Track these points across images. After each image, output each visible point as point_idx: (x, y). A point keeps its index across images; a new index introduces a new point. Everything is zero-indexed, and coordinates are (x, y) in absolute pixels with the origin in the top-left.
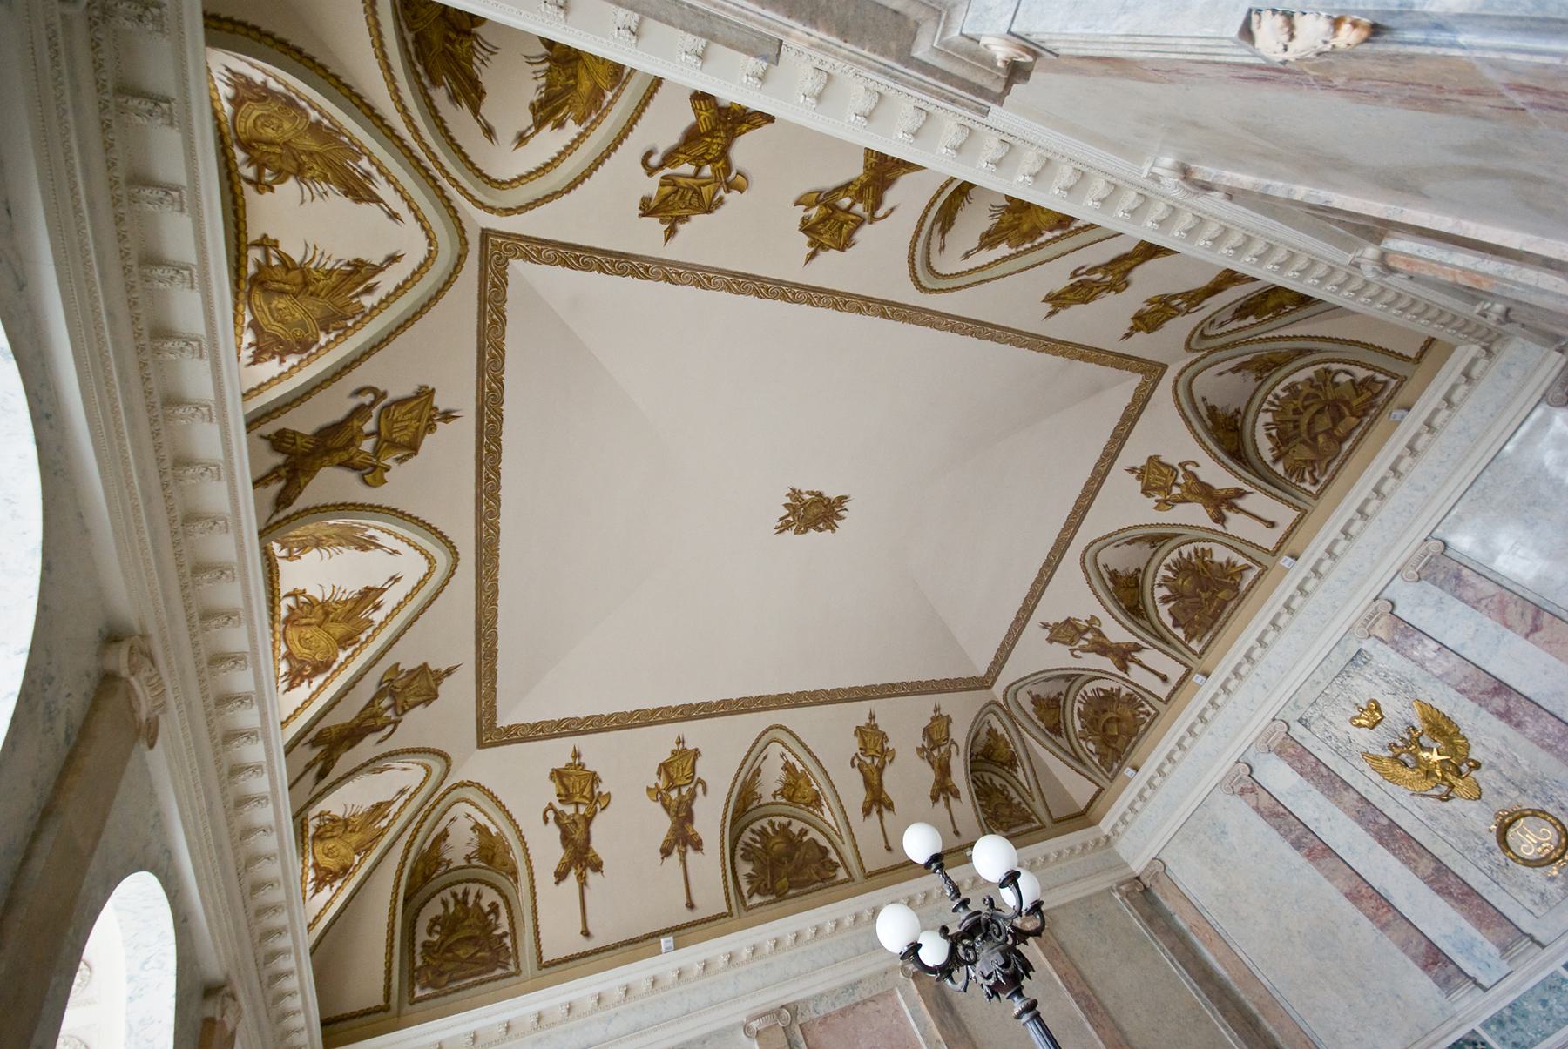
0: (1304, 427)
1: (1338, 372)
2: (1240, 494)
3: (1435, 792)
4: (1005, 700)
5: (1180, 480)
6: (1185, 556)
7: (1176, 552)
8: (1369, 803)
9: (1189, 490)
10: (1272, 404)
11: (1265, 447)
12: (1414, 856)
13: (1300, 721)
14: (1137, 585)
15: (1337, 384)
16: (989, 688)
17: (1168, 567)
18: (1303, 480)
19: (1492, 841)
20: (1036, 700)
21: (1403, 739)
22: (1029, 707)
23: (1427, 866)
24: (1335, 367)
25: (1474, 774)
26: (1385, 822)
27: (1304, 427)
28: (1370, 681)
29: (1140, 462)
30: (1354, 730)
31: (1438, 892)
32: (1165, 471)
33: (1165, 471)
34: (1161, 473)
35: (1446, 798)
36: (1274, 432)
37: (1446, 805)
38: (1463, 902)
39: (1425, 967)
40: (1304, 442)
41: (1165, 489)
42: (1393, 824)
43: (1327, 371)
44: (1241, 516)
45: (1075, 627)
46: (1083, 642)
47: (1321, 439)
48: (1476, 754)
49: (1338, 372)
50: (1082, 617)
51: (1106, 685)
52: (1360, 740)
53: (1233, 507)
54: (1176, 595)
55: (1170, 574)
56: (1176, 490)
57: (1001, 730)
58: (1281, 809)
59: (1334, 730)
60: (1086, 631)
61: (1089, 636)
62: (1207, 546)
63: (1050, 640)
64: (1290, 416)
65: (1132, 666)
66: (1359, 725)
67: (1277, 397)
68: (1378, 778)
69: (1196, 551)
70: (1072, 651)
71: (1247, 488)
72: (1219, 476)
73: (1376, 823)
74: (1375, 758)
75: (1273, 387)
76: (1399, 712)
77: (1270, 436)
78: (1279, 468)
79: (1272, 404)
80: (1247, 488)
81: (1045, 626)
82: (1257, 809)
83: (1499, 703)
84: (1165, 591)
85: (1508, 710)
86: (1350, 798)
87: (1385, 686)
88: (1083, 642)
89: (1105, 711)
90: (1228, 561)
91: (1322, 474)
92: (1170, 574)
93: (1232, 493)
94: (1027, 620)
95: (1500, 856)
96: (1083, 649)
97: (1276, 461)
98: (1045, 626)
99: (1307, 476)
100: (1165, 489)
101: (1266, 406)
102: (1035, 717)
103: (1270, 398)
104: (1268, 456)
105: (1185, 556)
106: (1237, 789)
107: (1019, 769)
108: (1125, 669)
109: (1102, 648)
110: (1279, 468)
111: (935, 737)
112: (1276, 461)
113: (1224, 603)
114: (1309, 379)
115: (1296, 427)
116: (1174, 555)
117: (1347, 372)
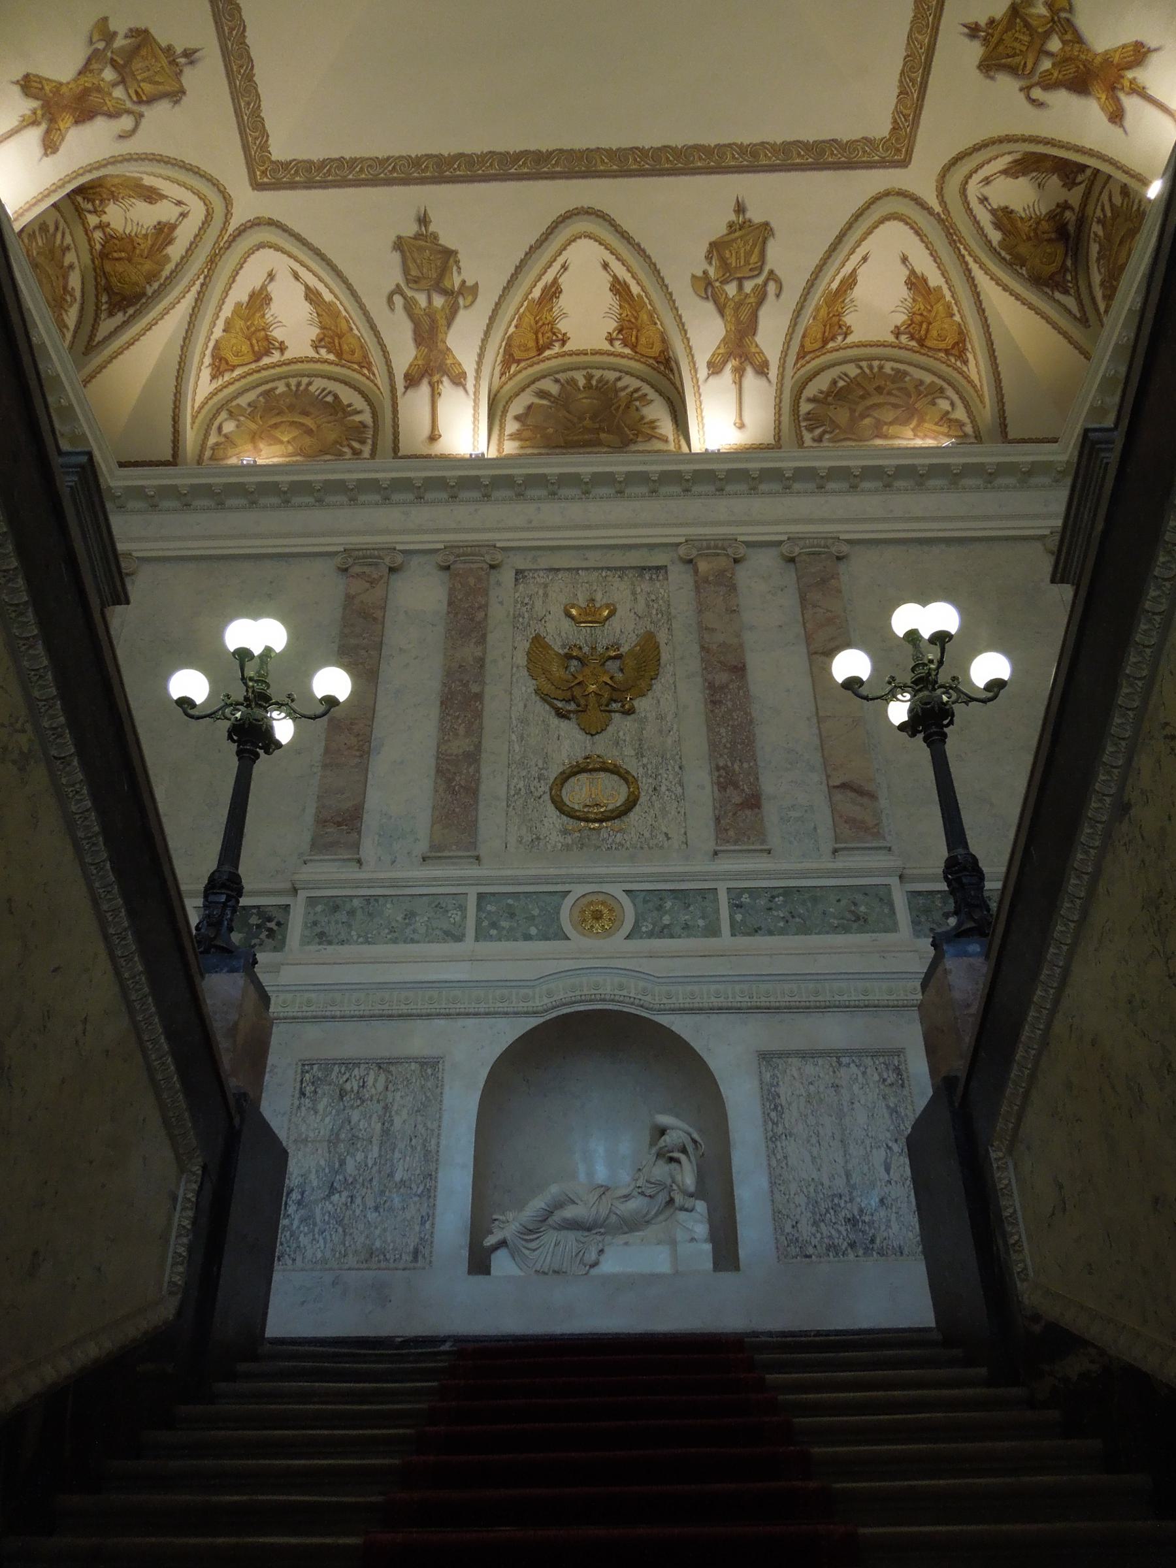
0: (869, 402)
1: (947, 398)
2: (762, 370)
3: (560, 705)
4: (241, 231)
5: (748, 286)
6: (620, 384)
7: (617, 374)
8: (482, 666)
9: (739, 305)
10: (871, 367)
11: (821, 384)
12: (462, 731)
13: (518, 572)
14: (540, 350)
15: (934, 404)
16: (258, 186)
17: (589, 378)
18: (810, 429)
19: (553, 773)
20: (260, 299)
21: (594, 649)
22: (240, 293)
23: (458, 746)
24: (950, 392)
25: (617, 717)
26: (475, 688)
27: (869, 402)
28: (634, 593)
29: (755, 215)
30: (557, 610)
31: (439, 771)
32: (754, 258)
33: (754, 258)
34: (749, 254)
35: (561, 715)
36: (841, 384)
37: (555, 721)
38: (454, 793)
39: (321, 822)
40: (853, 411)
41: (728, 272)
42: (479, 697)
43: (942, 390)
44: (733, 389)
45: (444, 271)
46: (422, 299)
47: (867, 421)
48: (642, 705)
49: (947, 398)
50: (468, 271)
51: (347, 396)
52: (551, 627)
53: (739, 372)
54: (563, 401)
55: (582, 382)
56: (731, 289)
57: (175, 251)
58: (379, 614)
59: (538, 603)
60: (445, 292)
61: (439, 301)
62: (652, 394)
63: (400, 245)
64: (871, 389)
65: (425, 388)
66: (569, 615)
67: (881, 368)
68: (521, 659)
69: (637, 390)
70: (398, 290)
71: (773, 372)
72: (771, 334)
73: (466, 685)
74: (547, 647)
75: (888, 359)
76: (624, 630)
77: (834, 382)
78: (805, 407)
79: (871, 367)
80: (773, 372)
81: (423, 220)
82: (349, 598)
83: (722, 677)
84: (554, 389)
85: (723, 687)
86: (469, 651)
87: (641, 606)
88: (422, 299)
89: (306, 413)
90: (653, 422)
91: (830, 440)
92: (582, 382)
93: (758, 360)
94: (422, 181)
95: (544, 788)
96: (409, 307)
97: (809, 400)
98: (423, 220)
99: (818, 432)
100: (728, 272)
101: (864, 364)
102: (227, 311)
103: (876, 363)
104: (811, 390)
105: (620, 384)
106: (357, 569)
107: (120, 318)
108: (412, 381)
109: (428, 333)
110: (805, 407)
111: (137, 64)
112: (809, 400)
113: (598, 443)
114: (921, 382)
115: (863, 397)
116: (611, 376)
117: (952, 404)
